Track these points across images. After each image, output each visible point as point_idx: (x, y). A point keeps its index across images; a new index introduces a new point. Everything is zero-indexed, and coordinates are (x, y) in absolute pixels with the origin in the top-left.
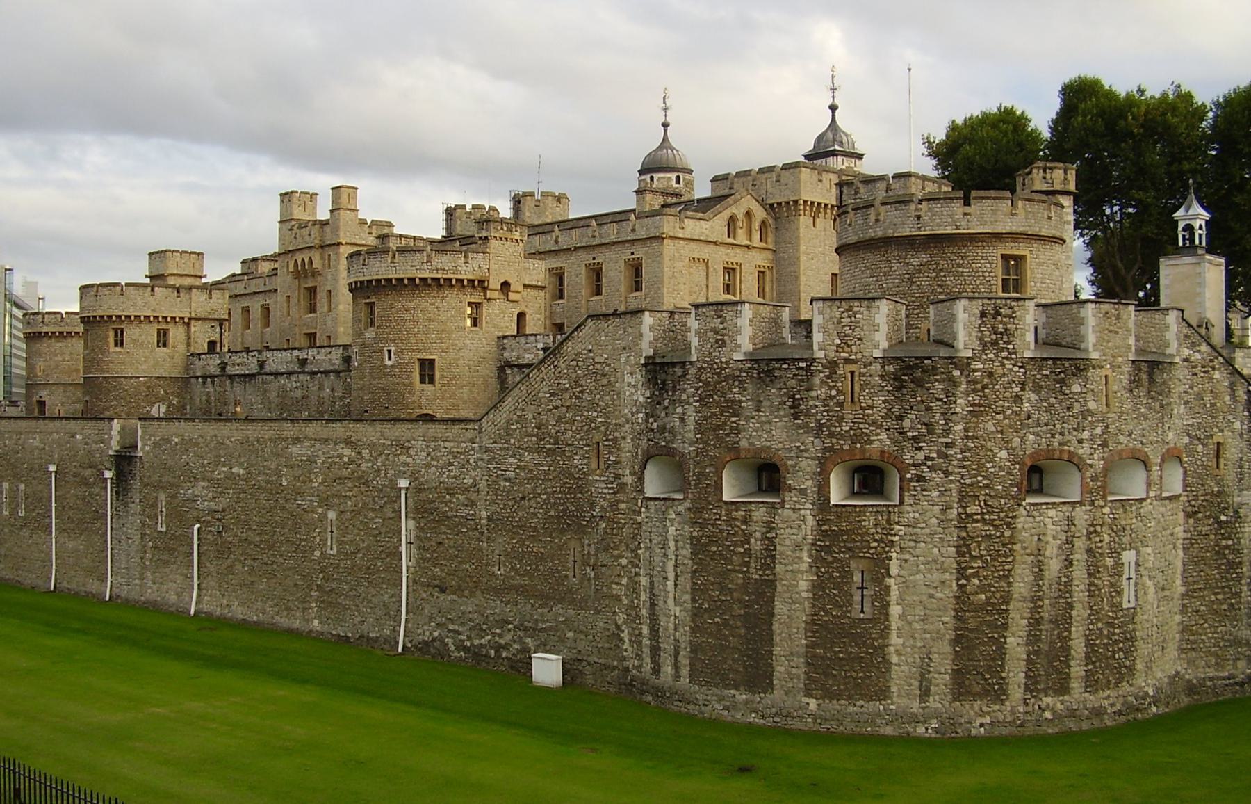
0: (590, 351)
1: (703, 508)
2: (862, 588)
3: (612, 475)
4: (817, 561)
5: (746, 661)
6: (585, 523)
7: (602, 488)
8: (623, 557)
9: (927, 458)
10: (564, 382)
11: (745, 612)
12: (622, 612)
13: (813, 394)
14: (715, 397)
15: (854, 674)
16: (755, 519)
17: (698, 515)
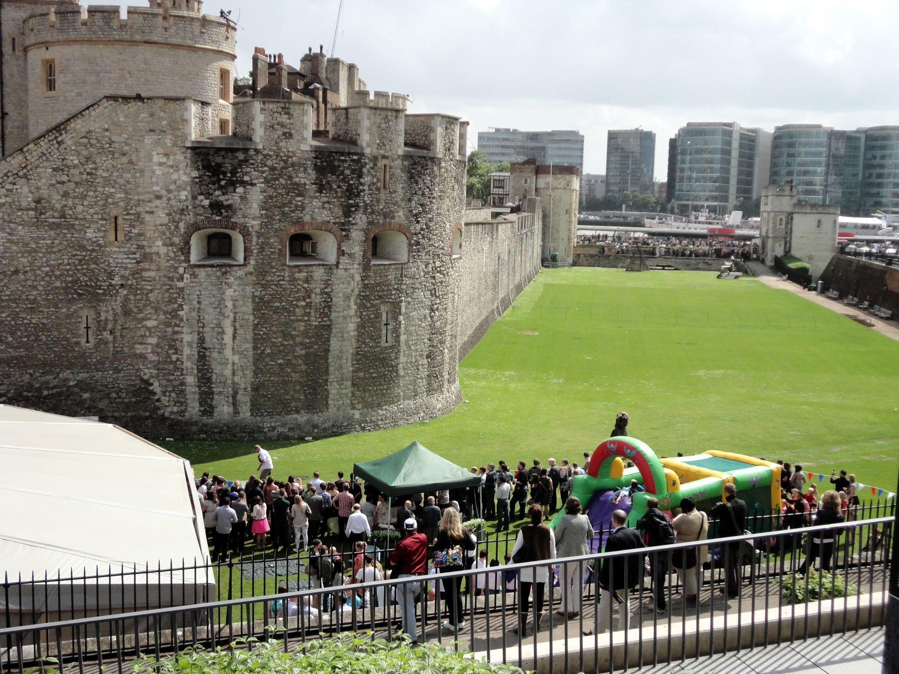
0: (107, 130)
1: (266, 272)
2: (387, 324)
3: (135, 246)
4: (361, 306)
5: (305, 390)
6: (101, 291)
7: (122, 259)
8: (150, 319)
9: (422, 229)
10: (71, 158)
11: (306, 353)
12: (148, 368)
13: (362, 181)
14: (281, 180)
15: (381, 387)
16: (316, 278)
17: (261, 278)
